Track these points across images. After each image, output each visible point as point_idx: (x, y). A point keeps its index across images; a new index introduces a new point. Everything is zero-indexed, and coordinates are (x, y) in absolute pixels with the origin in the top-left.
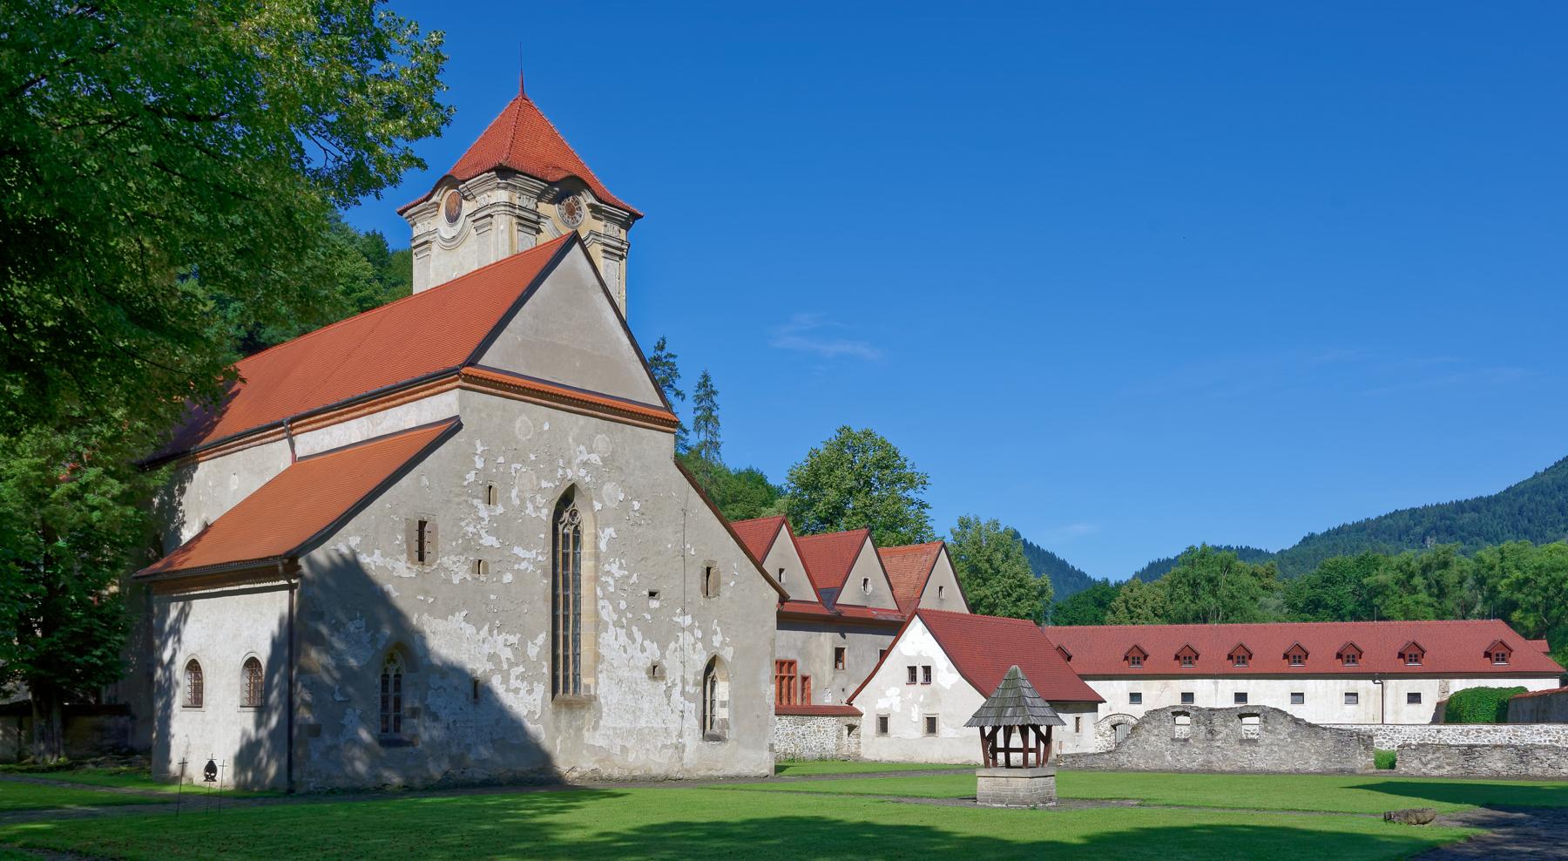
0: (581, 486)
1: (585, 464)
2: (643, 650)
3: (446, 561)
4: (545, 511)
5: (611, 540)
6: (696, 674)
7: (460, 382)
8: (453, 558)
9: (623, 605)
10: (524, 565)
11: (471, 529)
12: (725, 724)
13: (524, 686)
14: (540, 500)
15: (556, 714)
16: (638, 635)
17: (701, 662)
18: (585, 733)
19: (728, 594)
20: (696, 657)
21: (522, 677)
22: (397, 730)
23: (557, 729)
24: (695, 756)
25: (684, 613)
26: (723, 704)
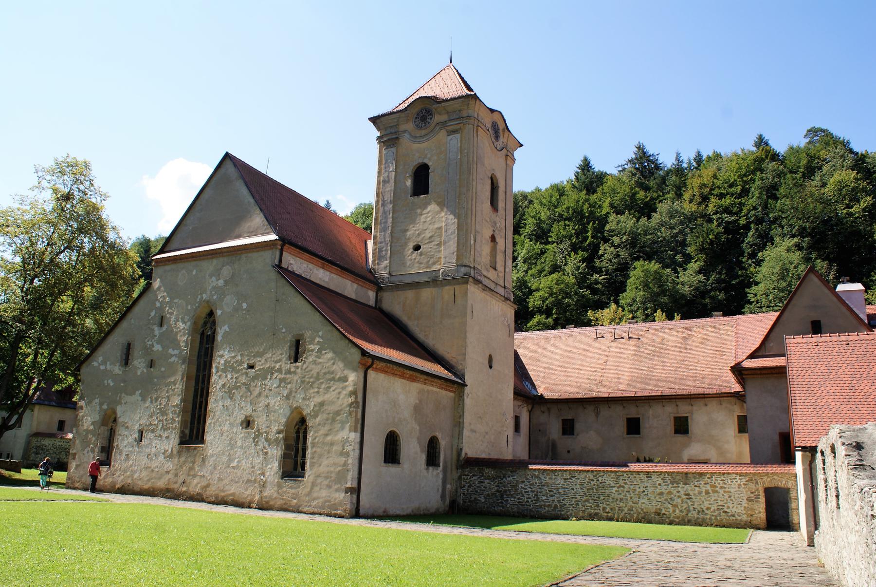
1: (214, 288)
5: (226, 334)
8: (139, 360)
11: (150, 343)
14: (187, 318)
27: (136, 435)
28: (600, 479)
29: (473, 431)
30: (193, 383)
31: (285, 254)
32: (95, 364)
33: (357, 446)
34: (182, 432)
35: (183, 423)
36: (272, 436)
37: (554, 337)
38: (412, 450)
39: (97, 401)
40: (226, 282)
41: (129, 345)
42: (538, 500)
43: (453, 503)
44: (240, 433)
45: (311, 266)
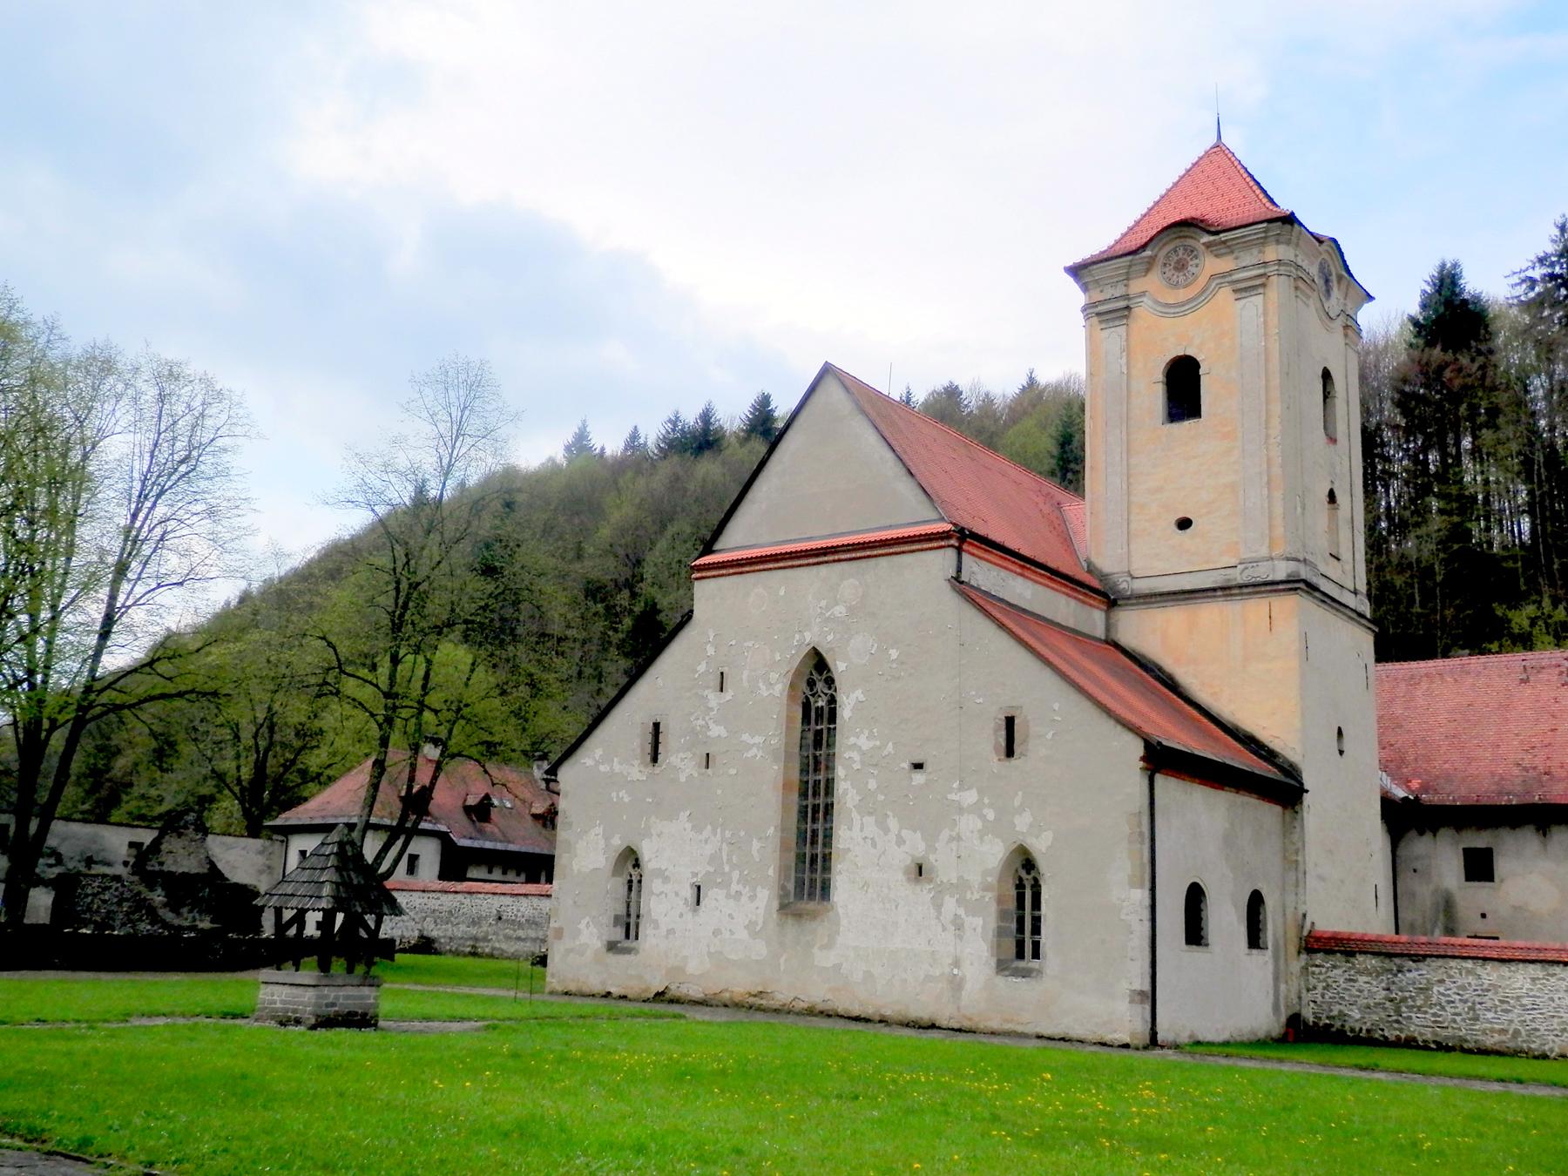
2: (900, 841)
4: (779, 687)
8: (682, 755)
9: (872, 784)
11: (701, 722)
13: (746, 891)
14: (774, 676)
16: (893, 823)
17: (994, 855)
18: (815, 950)
21: (743, 880)
27: (689, 894)
29: (1321, 878)
30: (795, 796)
31: (965, 556)
32: (589, 762)
33: (1146, 914)
34: (783, 888)
35: (783, 870)
37: (1427, 675)
38: (1225, 918)
39: (599, 830)
40: (851, 610)
41: (656, 726)
42: (1476, 1019)
43: (1294, 1020)
44: (903, 888)
45: (1004, 573)
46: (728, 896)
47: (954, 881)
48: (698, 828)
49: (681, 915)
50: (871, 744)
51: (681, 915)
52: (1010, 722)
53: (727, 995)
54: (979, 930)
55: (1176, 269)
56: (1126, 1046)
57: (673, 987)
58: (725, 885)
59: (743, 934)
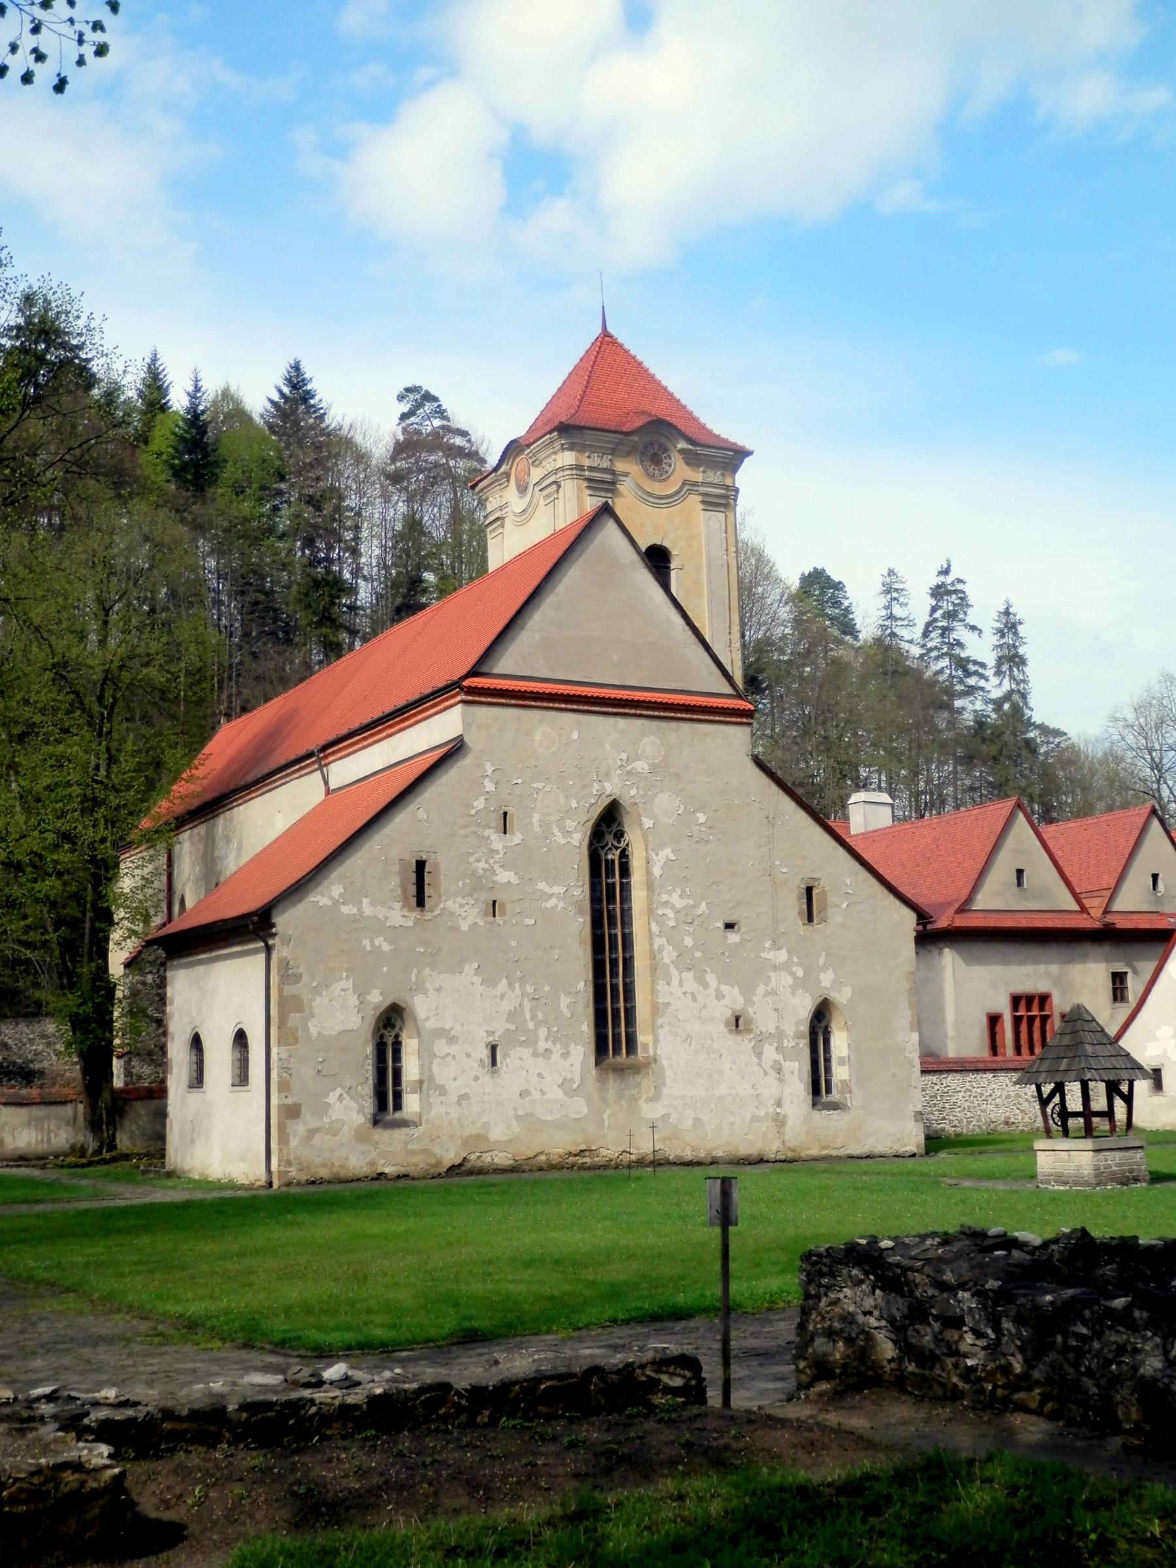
0: (625, 802)
2: (719, 996)
3: (451, 905)
5: (668, 864)
6: (798, 1023)
7: (462, 697)
8: (459, 900)
9: (688, 941)
10: (553, 902)
11: (482, 865)
12: (846, 1087)
13: (557, 1049)
14: (570, 824)
15: (602, 1081)
16: (711, 979)
17: (804, 1008)
18: (642, 1103)
19: (839, 919)
20: (797, 1001)
21: (552, 1037)
22: (398, 1106)
23: (604, 1100)
24: (800, 1127)
25: (776, 946)
26: (842, 1062)
27: (485, 1054)
28: (944, 1081)
32: (323, 901)
36: (789, 1043)
40: (654, 768)
41: (421, 865)
44: (726, 1040)
46: (535, 1054)
47: (773, 1031)
48: (490, 982)
49: (476, 1078)
50: (685, 902)
51: (476, 1078)
52: (809, 890)
53: (543, 1158)
54: (796, 1073)
55: (652, 460)
56: (914, 1155)
57: (473, 1157)
58: (530, 1042)
59: (559, 1094)
